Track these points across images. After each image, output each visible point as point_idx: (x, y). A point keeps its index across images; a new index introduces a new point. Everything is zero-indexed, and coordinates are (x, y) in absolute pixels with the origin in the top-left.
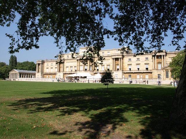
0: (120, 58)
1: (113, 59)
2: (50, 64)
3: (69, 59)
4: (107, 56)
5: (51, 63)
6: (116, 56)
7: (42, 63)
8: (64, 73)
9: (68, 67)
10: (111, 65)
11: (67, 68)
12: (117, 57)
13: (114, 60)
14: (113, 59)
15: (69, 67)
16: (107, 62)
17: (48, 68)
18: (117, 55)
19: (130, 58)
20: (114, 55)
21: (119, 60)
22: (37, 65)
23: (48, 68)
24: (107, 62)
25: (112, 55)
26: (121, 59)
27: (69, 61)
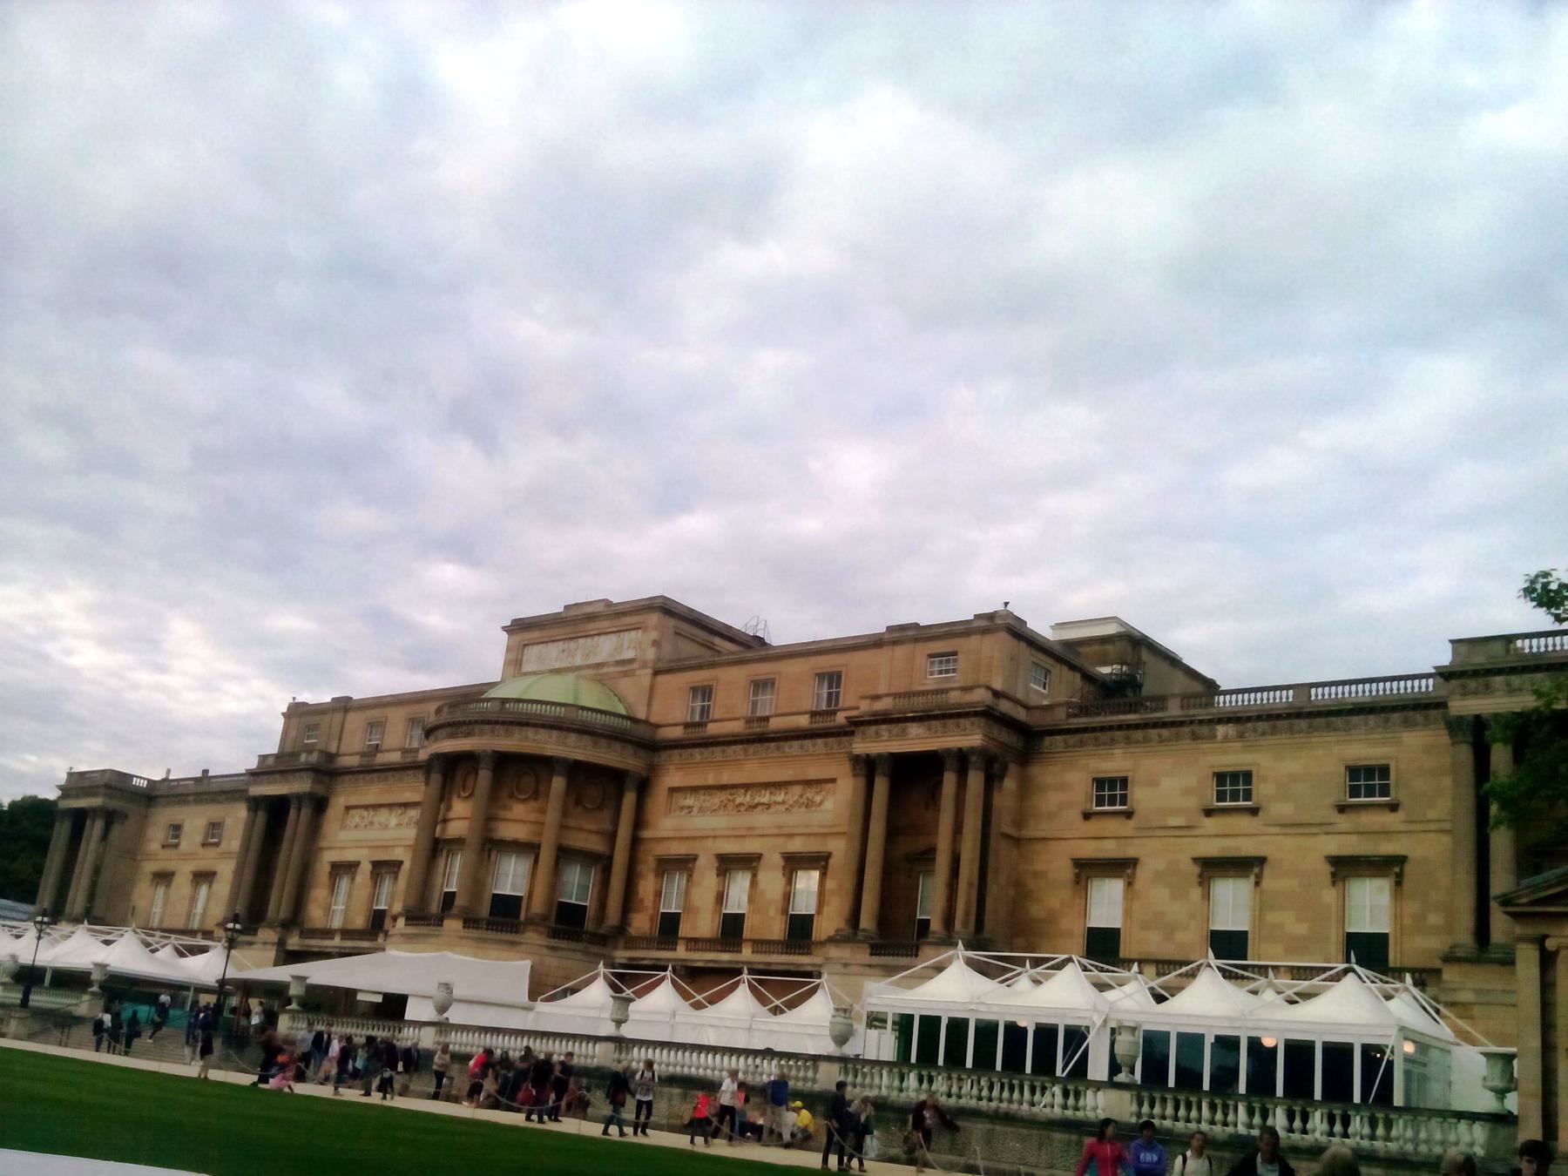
0: (962, 759)
1: (867, 767)
2: (194, 820)
3: (381, 759)
4: (803, 721)
5: (211, 812)
6: (914, 729)
7: (114, 804)
8: (294, 942)
9: (350, 867)
10: (840, 850)
11: (344, 883)
12: (917, 740)
13: (881, 786)
14: (867, 767)
15: (366, 868)
16: (796, 818)
17: (164, 877)
18: (920, 703)
19: (1114, 762)
20: (885, 704)
21: (949, 780)
22: (61, 833)
23: (164, 877)
24: (796, 818)
25: (865, 706)
26: (975, 780)
27: (373, 792)
